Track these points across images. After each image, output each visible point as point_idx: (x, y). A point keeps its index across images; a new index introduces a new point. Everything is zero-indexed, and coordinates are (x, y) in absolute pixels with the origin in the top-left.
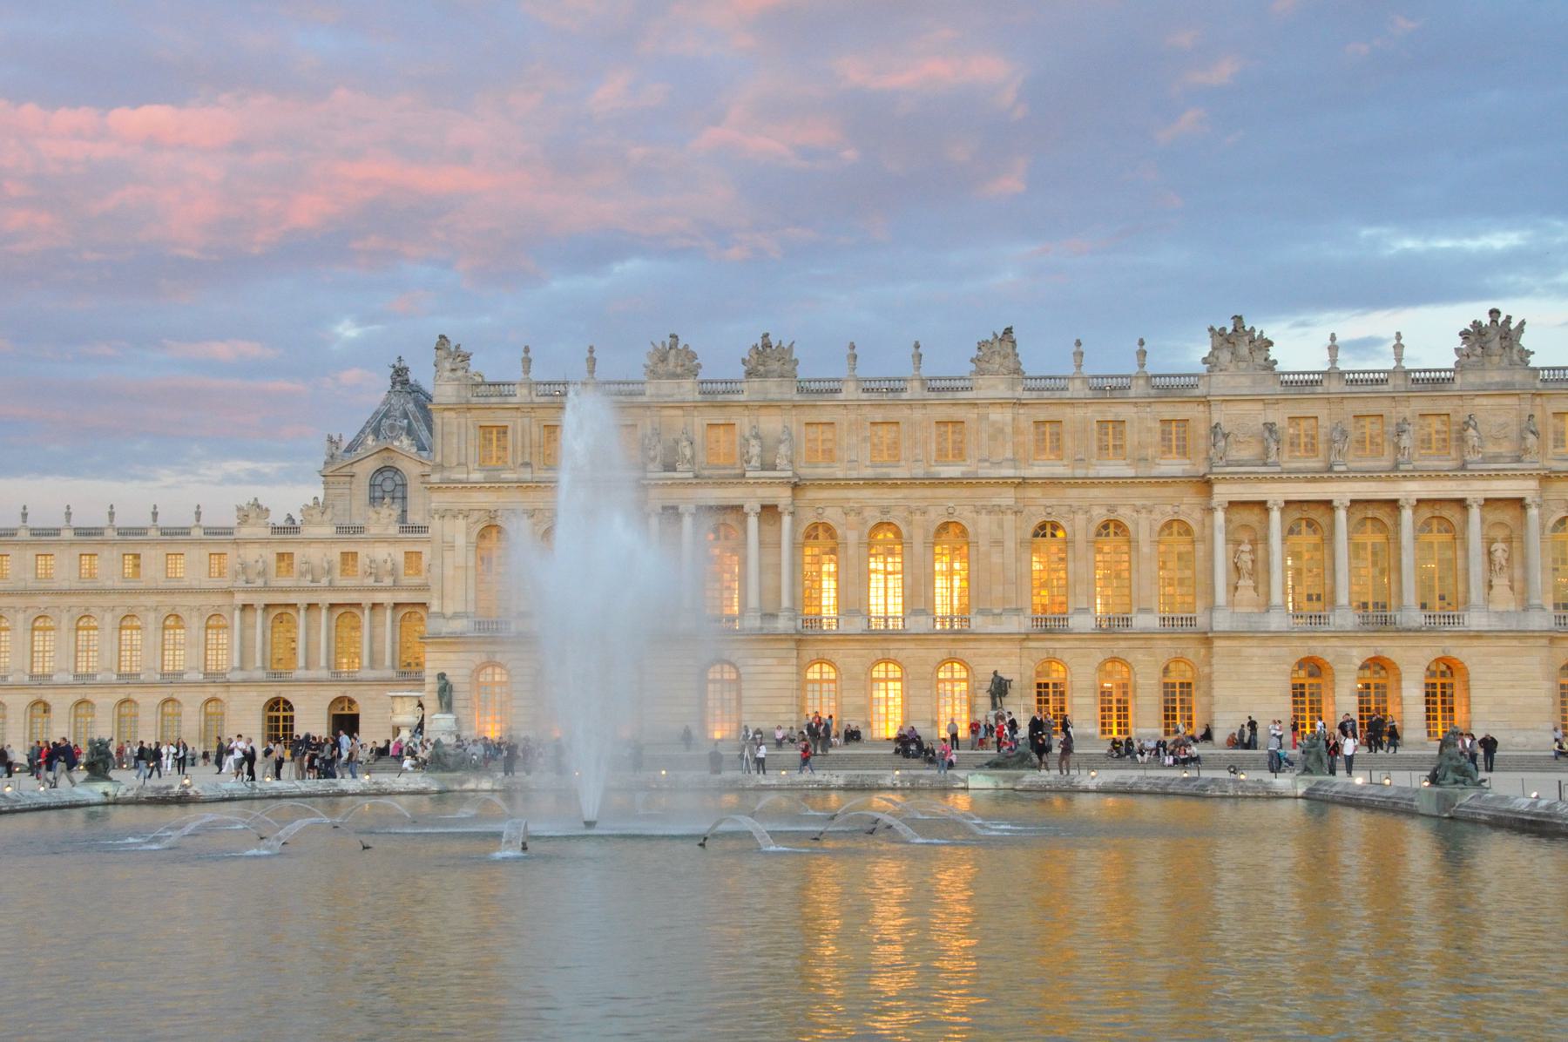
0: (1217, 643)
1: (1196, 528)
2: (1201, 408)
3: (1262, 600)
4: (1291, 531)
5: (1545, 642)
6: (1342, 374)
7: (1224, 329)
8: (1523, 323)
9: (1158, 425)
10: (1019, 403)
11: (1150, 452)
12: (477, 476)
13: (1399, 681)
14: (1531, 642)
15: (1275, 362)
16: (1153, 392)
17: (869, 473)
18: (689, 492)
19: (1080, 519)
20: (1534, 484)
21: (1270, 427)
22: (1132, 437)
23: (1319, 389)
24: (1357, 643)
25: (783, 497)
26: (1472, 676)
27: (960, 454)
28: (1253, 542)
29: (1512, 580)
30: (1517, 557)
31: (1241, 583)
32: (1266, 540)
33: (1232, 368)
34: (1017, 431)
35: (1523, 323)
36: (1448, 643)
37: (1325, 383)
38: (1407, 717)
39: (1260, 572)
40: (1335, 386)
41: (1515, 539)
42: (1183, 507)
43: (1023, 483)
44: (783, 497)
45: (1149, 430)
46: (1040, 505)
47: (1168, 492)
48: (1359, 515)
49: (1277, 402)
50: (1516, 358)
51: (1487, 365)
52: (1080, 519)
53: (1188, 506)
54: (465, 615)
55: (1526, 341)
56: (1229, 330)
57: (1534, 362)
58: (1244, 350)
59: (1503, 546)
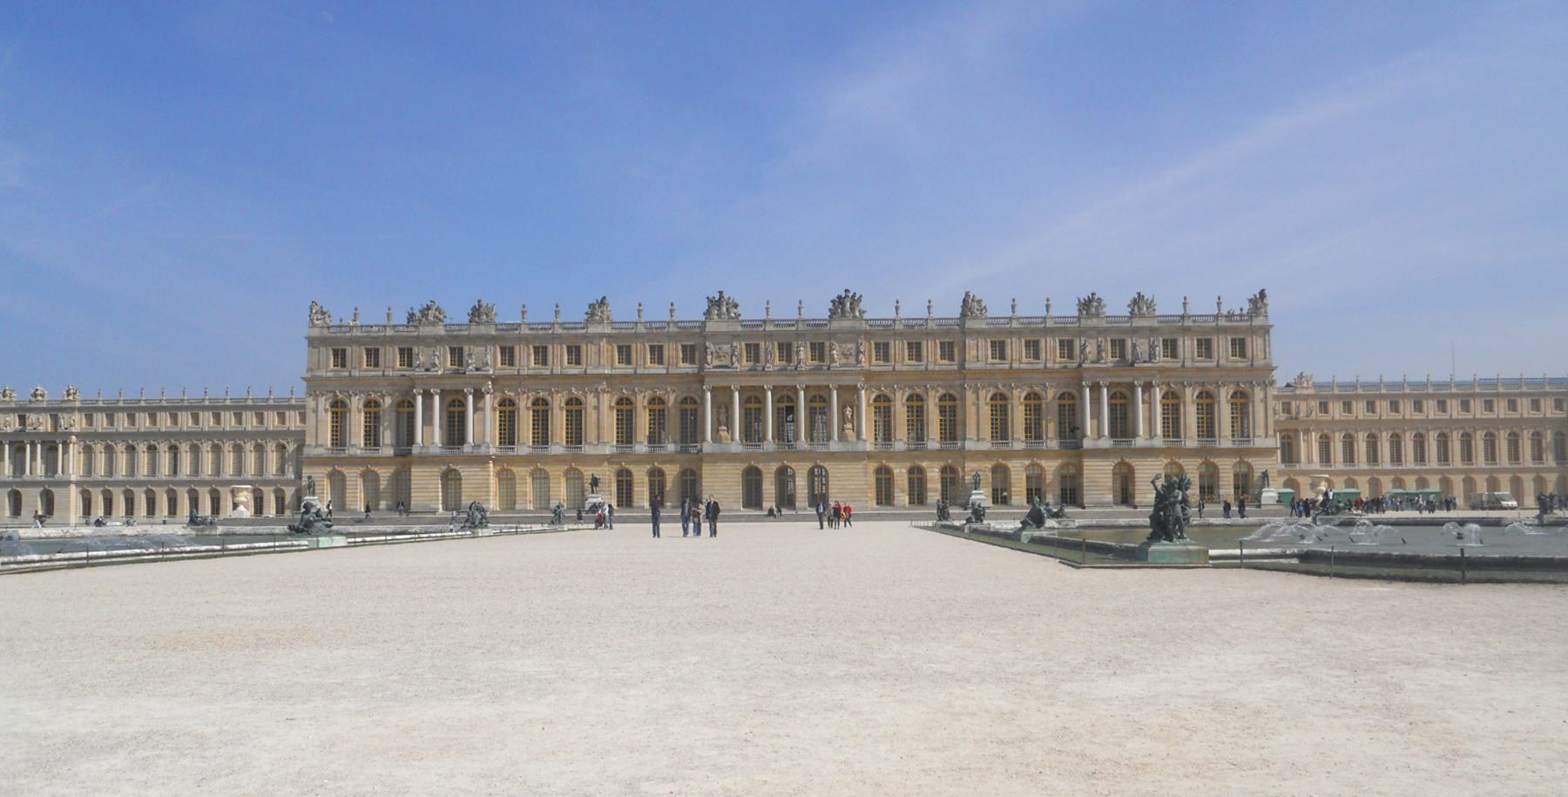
40: (770, 328)
41: (856, 406)
43: (609, 378)
55: (862, 306)
57: (866, 316)
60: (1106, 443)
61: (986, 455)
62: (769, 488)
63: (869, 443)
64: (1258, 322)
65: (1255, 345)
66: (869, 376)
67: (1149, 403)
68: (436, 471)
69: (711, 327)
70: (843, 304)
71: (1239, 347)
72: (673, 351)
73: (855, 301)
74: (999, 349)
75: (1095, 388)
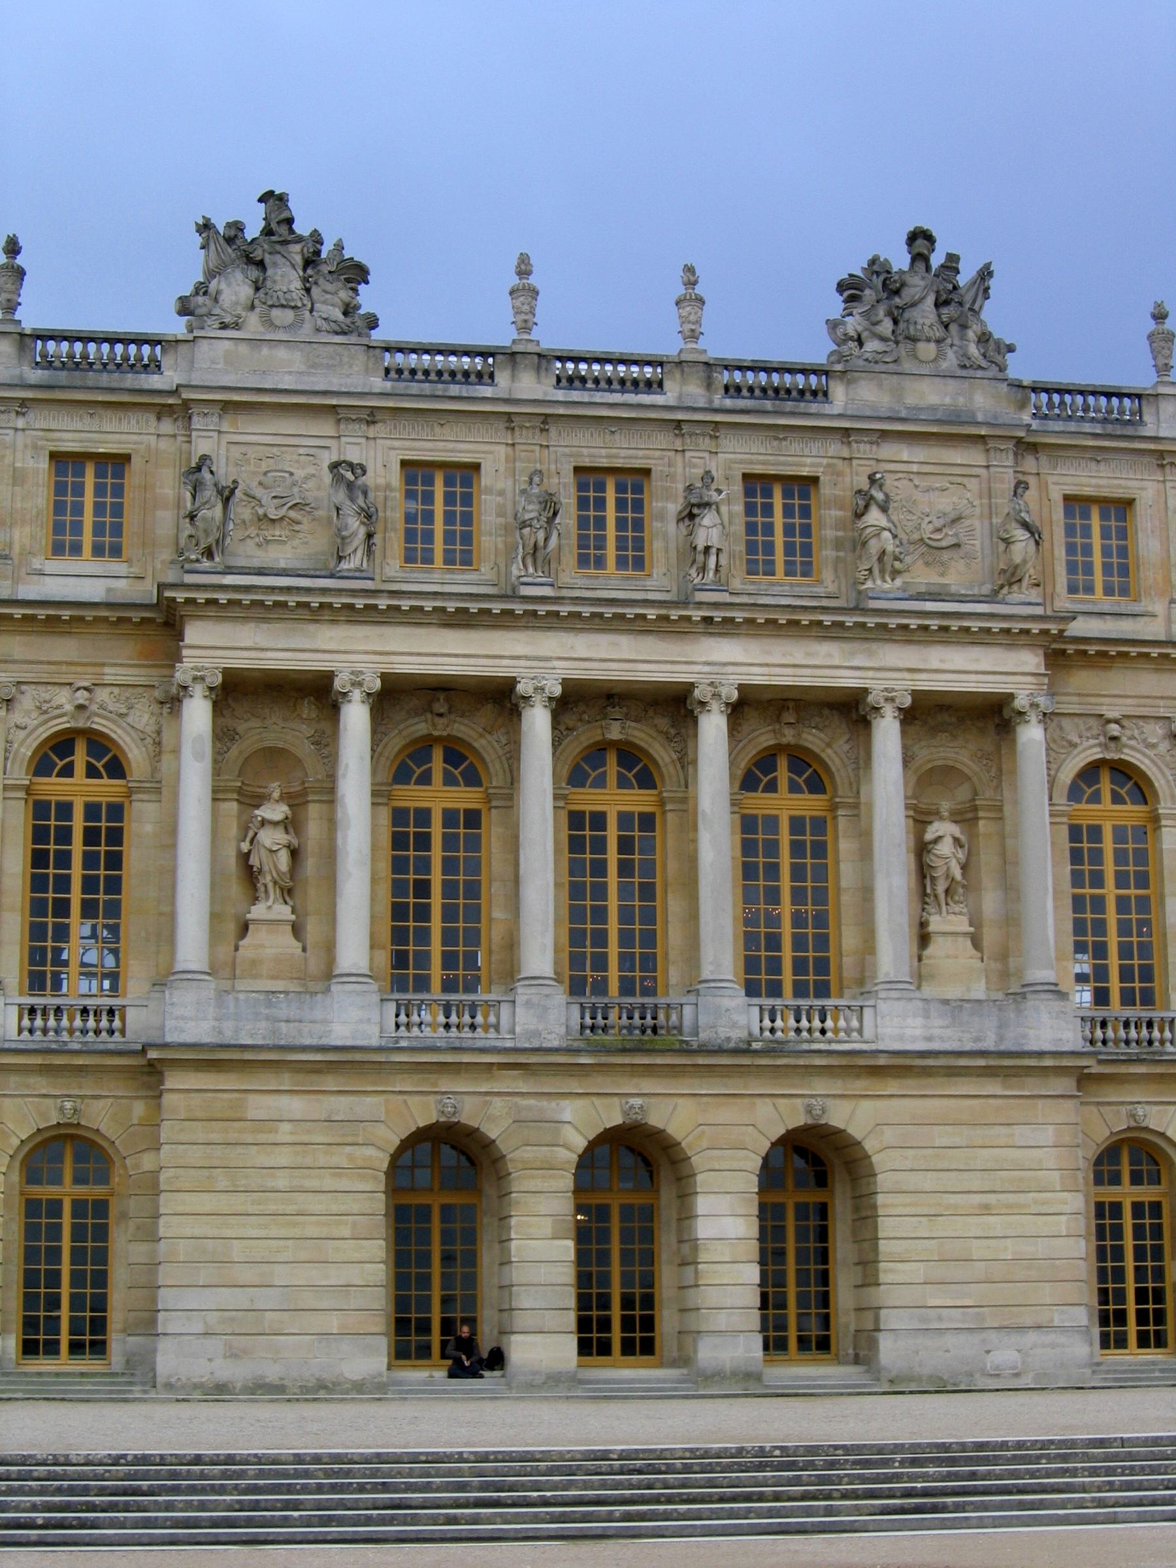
0: (173, 1080)
1: (135, 755)
2: (167, 426)
3: (315, 964)
4: (402, 775)
5: (1066, 1085)
6: (543, 359)
7: (238, 227)
8: (986, 273)
9: (44, 464)
11: (20, 536)
13: (685, 1196)
14: (1032, 1086)
15: (372, 322)
16: (36, 376)
20: (1031, 660)
21: (346, 474)
23: (486, 391)
24: (575, 1086)
26: (884, 1180)
28: (296, 801)
29: (975, 921)
30: (987, 858)
31: (258, 911)
32: (329, 792)
33: (253, 324)
35: (986, 273)
36: (821, 1086)
37: (502, 378)
38: (708, 1296)
39: (302, 880)
40: (530, 386)
42: (102, 695)
45: (18, 477)
47: (63, 649)
48: (586, 736)
49: (372, 417)
50: (973, 350)
51: (907, 366)
53: (106, 688)
55: (995, 316)
56: (253, 230)
58: (286, 277)
59: (955, 829)
62: (537, 1252)
69: (216, 364)
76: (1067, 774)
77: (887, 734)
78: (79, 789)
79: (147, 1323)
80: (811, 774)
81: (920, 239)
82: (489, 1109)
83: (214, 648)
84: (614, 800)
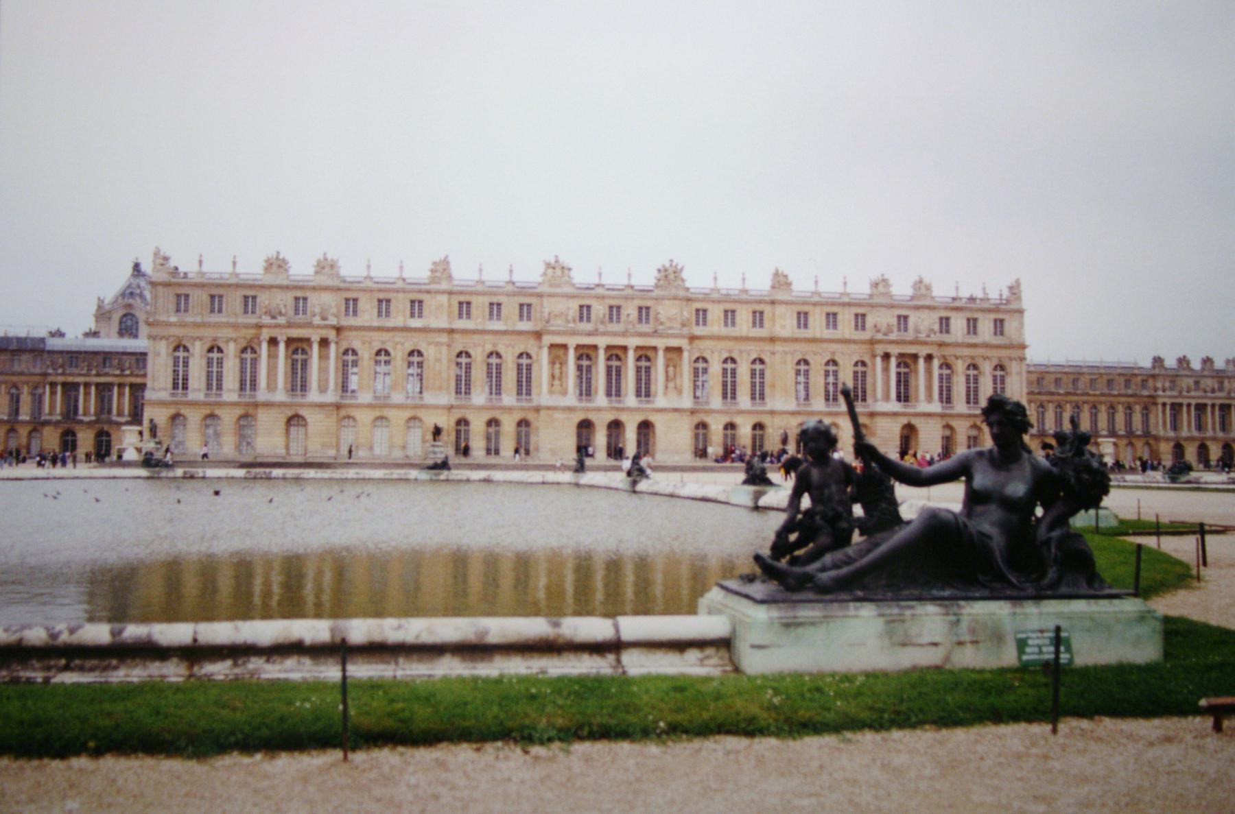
10: (450, 293)
12: (173, 319)
17: (376, 323)
18: (284, 331)
19: (479, 350)
22: (504, 310)
25: (332, 335)
27: (420, 316)
32: (566, 362)
34: (450, 306)
40: (600, 291)
43: (451, 331)
44: (332, 335)
46: (460, 343)
47: (522, 337)
52: (479, 350)
53: (530, 345)
54: (165, 389)
55: (684, 275)
57: (688, 284)
60: (894, 406)
61: (793, 413)
63: (687, 402)
64: (1013, 306)
65: (1010, 326)
66: (692, 338)
67: (929, 371)
68: (280, 417)
70: (670, 275)
71: (999, 326)
72: (510, 307)
73: (677, 272)
74: (803, 319)
75: (886, 356)
76: (694, 358)
77: (661, 354)
78: (524, 361)
79: (537, 449)
80: (648, 359)
81: (671, 261)
82: (592, 416)
83: (547, 340)
84: (615, 363)
